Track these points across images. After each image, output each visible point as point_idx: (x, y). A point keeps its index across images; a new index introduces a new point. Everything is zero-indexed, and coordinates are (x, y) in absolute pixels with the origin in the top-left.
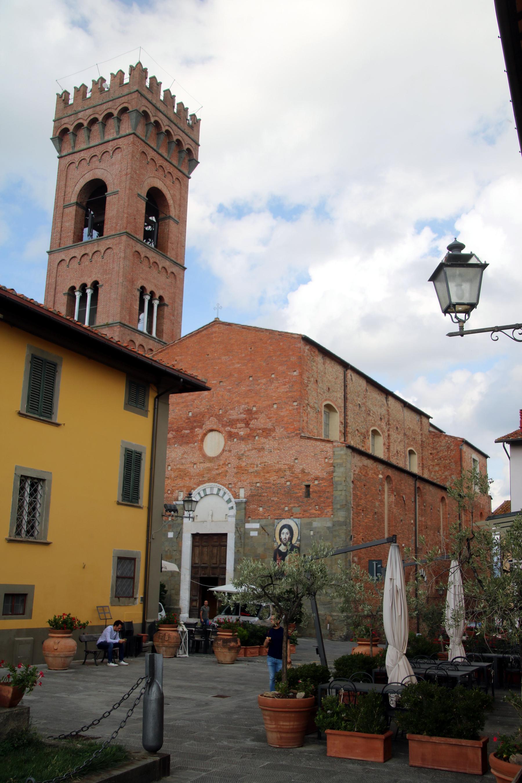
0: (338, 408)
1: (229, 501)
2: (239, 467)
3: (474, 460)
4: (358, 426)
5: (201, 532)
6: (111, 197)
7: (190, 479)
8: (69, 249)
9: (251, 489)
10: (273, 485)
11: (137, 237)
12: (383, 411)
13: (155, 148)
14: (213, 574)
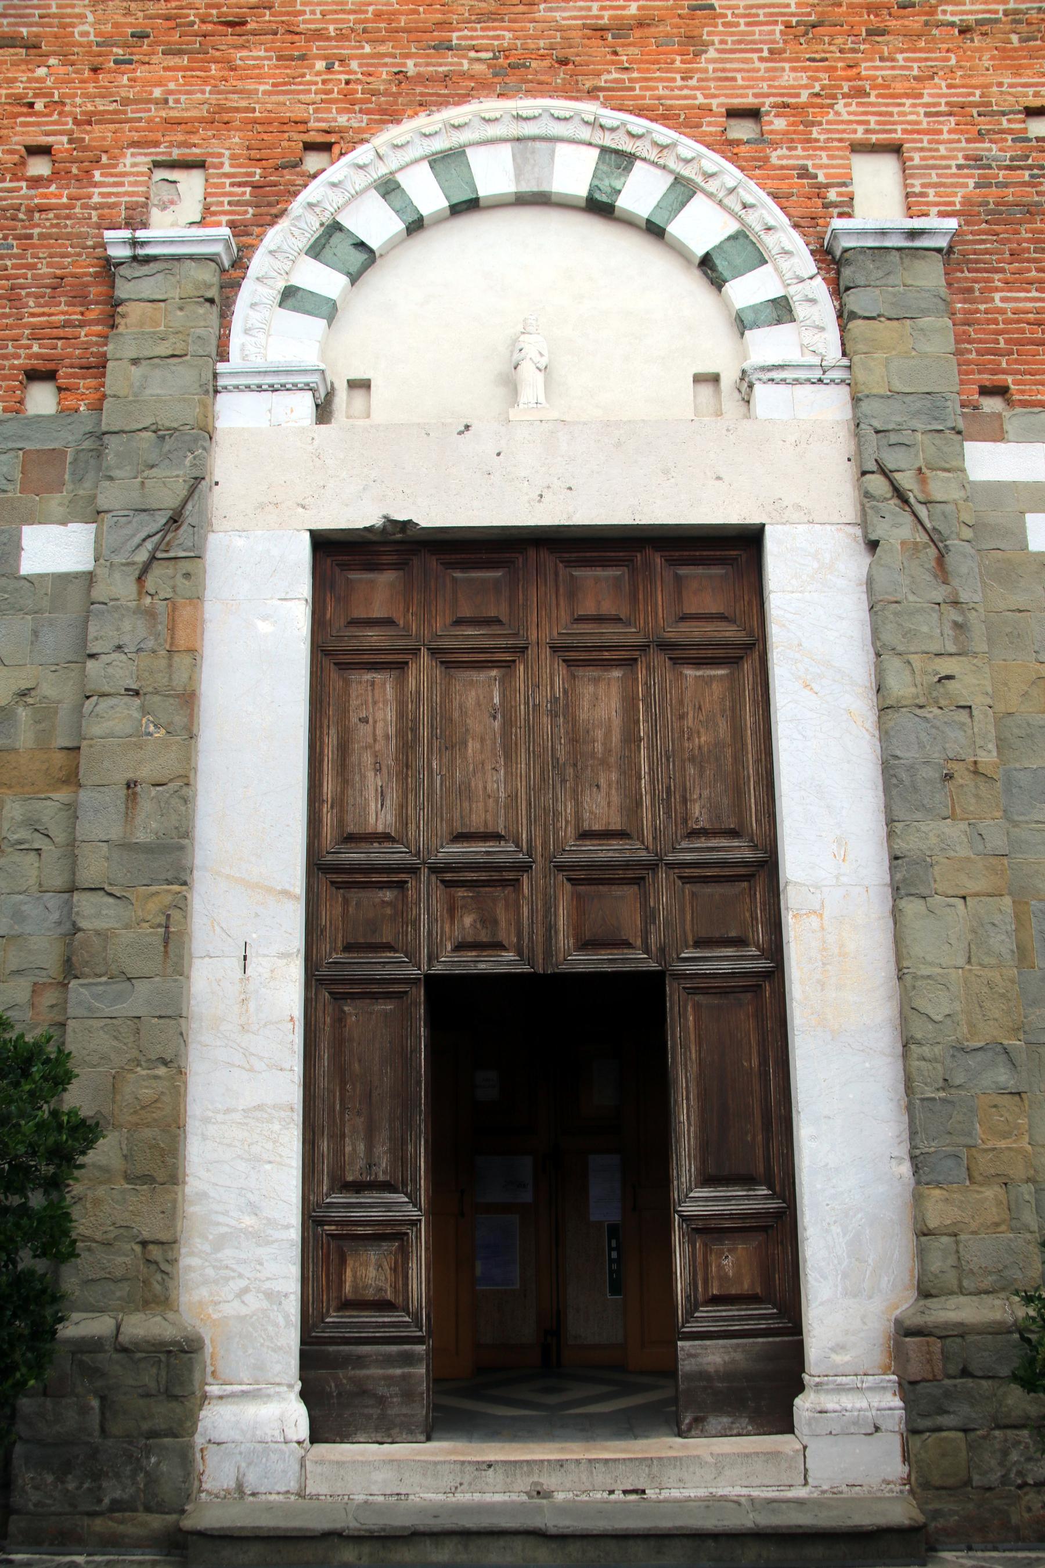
9: (976, 160)
14: (584, 945)
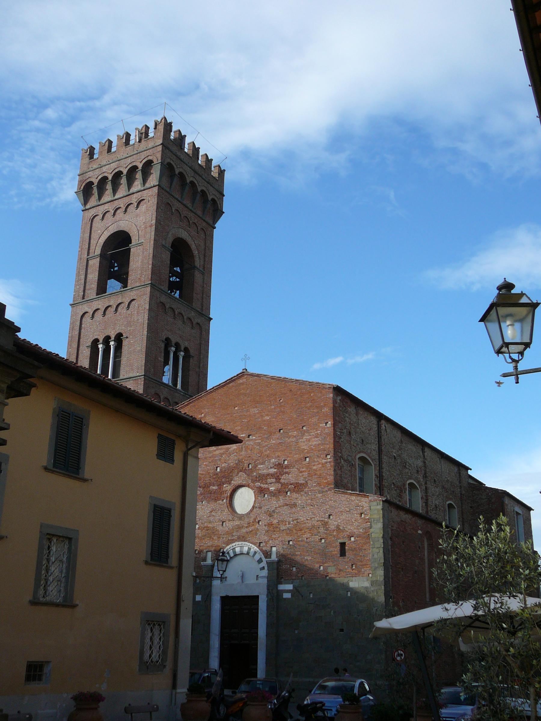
0: (372, 461)
1: (260, 561)
2: (270, 525)
3: (518, 514)
4: (394, 479)
5: (230, 595)
6: (135, 249)
7: (219, 538)
8: (92, 301)
10: (307, 542)
11: (162, 287)
12: (420, 463)
13: (179, 199)
